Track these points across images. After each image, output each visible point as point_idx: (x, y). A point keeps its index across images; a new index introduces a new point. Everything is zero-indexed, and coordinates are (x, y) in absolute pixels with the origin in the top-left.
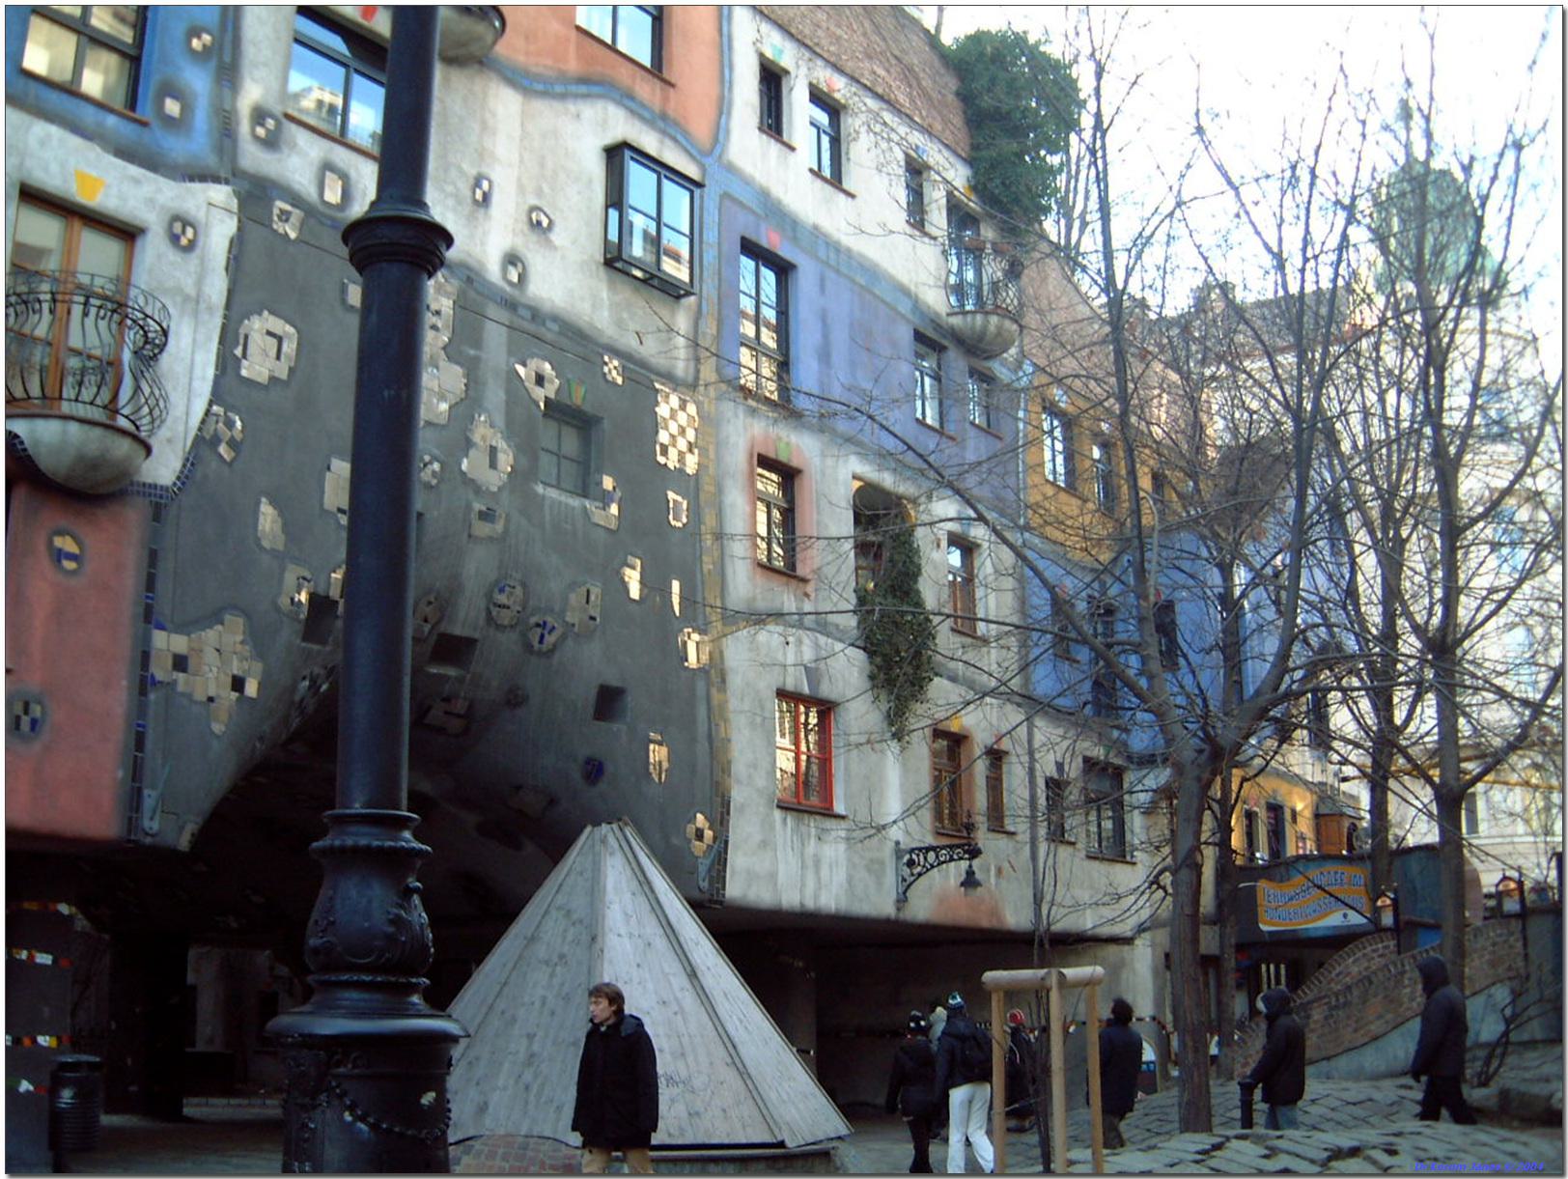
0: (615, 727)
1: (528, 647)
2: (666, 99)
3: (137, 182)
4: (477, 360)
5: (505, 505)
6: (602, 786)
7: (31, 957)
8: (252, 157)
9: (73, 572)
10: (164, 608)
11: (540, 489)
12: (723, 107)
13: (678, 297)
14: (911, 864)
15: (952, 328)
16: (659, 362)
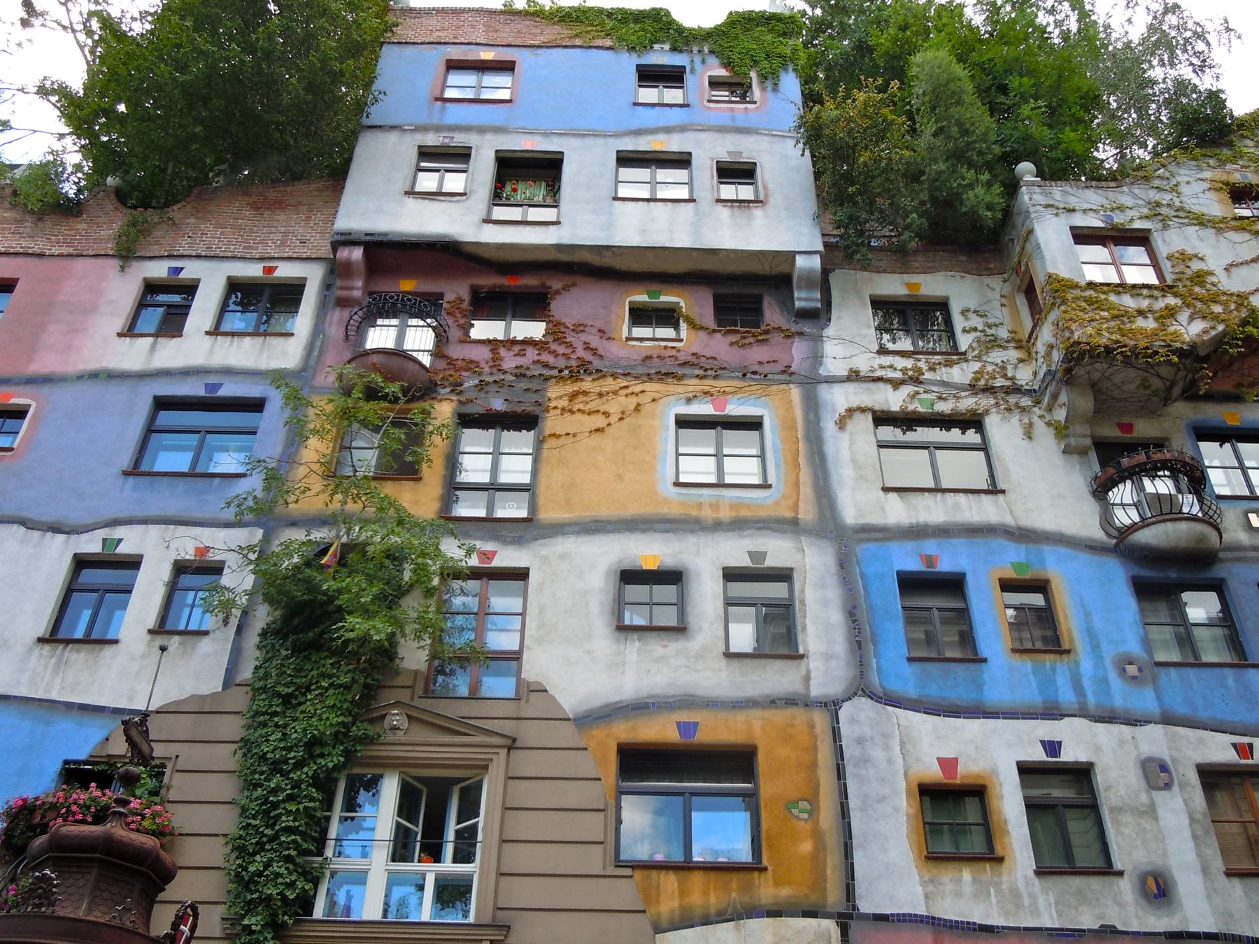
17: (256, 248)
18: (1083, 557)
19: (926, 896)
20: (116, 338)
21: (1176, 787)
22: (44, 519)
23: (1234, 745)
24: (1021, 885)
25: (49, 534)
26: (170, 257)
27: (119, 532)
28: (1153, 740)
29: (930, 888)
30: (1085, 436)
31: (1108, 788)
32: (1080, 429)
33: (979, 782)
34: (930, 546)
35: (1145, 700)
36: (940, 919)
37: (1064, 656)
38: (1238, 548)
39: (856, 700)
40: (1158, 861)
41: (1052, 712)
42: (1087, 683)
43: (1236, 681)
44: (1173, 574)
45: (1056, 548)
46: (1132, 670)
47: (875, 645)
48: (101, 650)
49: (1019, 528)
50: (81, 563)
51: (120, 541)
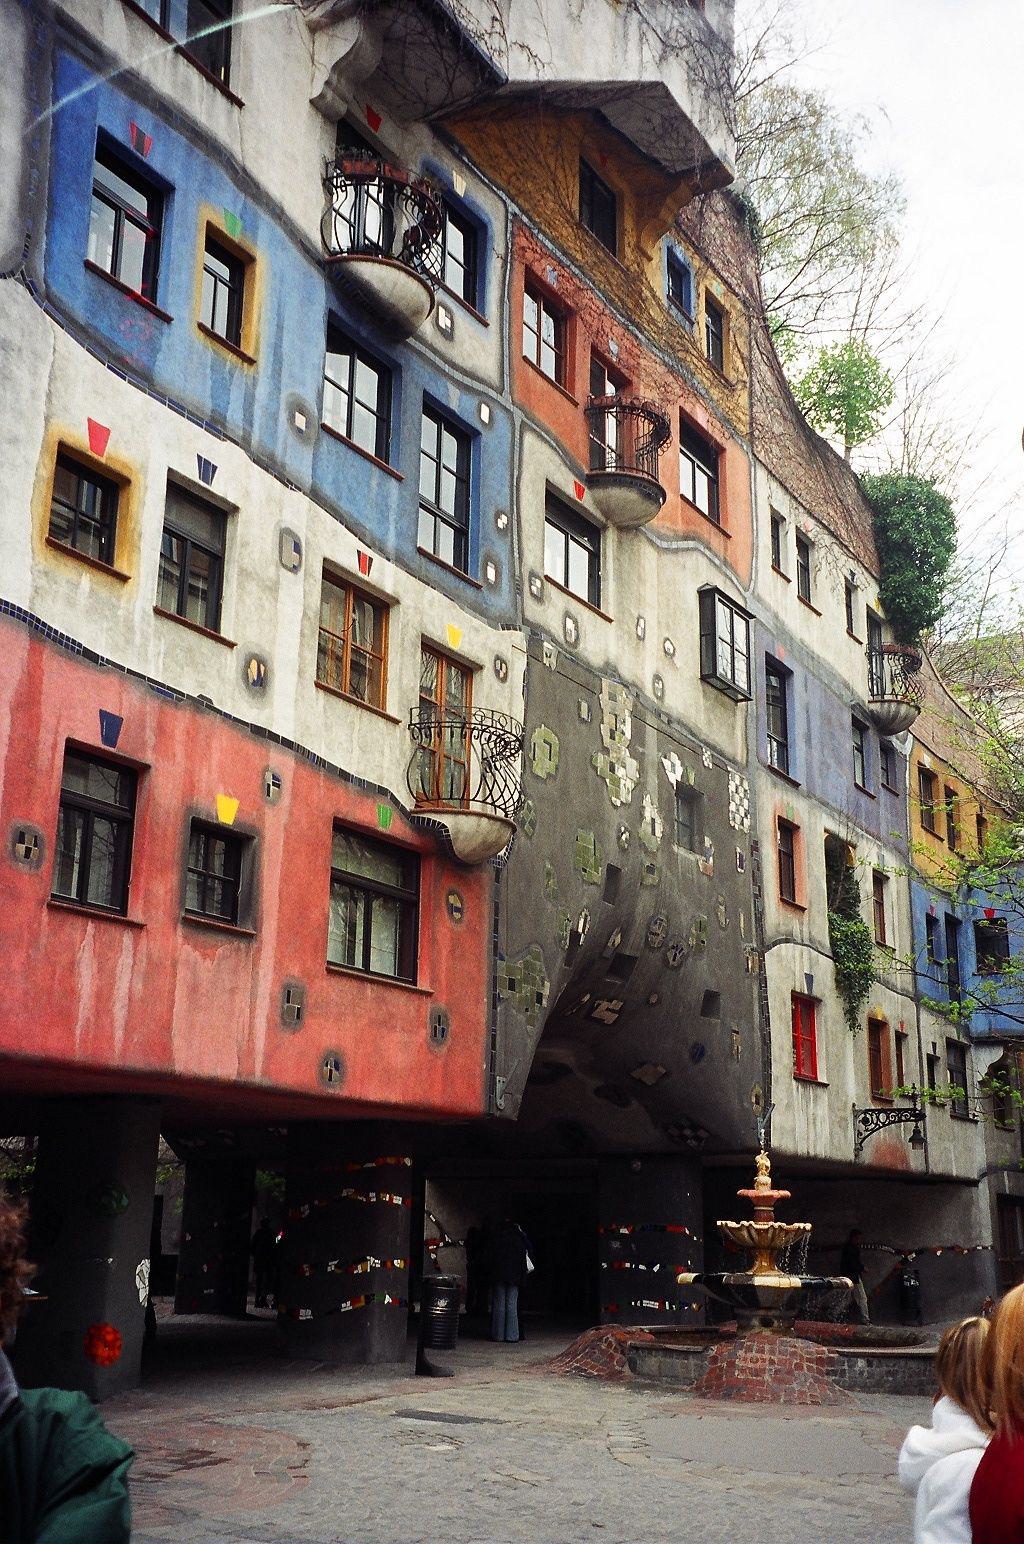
0: (714, 1021)
1: (665, 961)
2: (726, 549)
3: (477, 631)
4: (643, 754)
5: (660, 860)
6: (703, 1064)
7: (391, 1199)
8: (532, 610)
9: (459, 921)
10: (502, 946)
11: (675, 848)
12: (754, 549)
13: (737, 701)
14: (865, 1121)
15: (872, 711)
16: (728, 749)
18: (294, 253)
19: (36, 590)
21: (301, 573)
23: (359, 552)
24: (137, 618)
28: (298, 510)
29: (42, 582)
30: (344, 99)
31: (245, 545)
32: (344, 86)
33: (125, 473)
34: (146, 120)
35: (299, 461)
36: (44, 624)
37: (246, 364)
38: (421, 340)
39: (11, 281)
40: (264, 648)
41: (215, 426)
42: (258, 411)
43: (379, 485)
44: (364, 334)
45: (272, 222)
46: (300, 421)
47: (52, 215)
49: (244, 170)
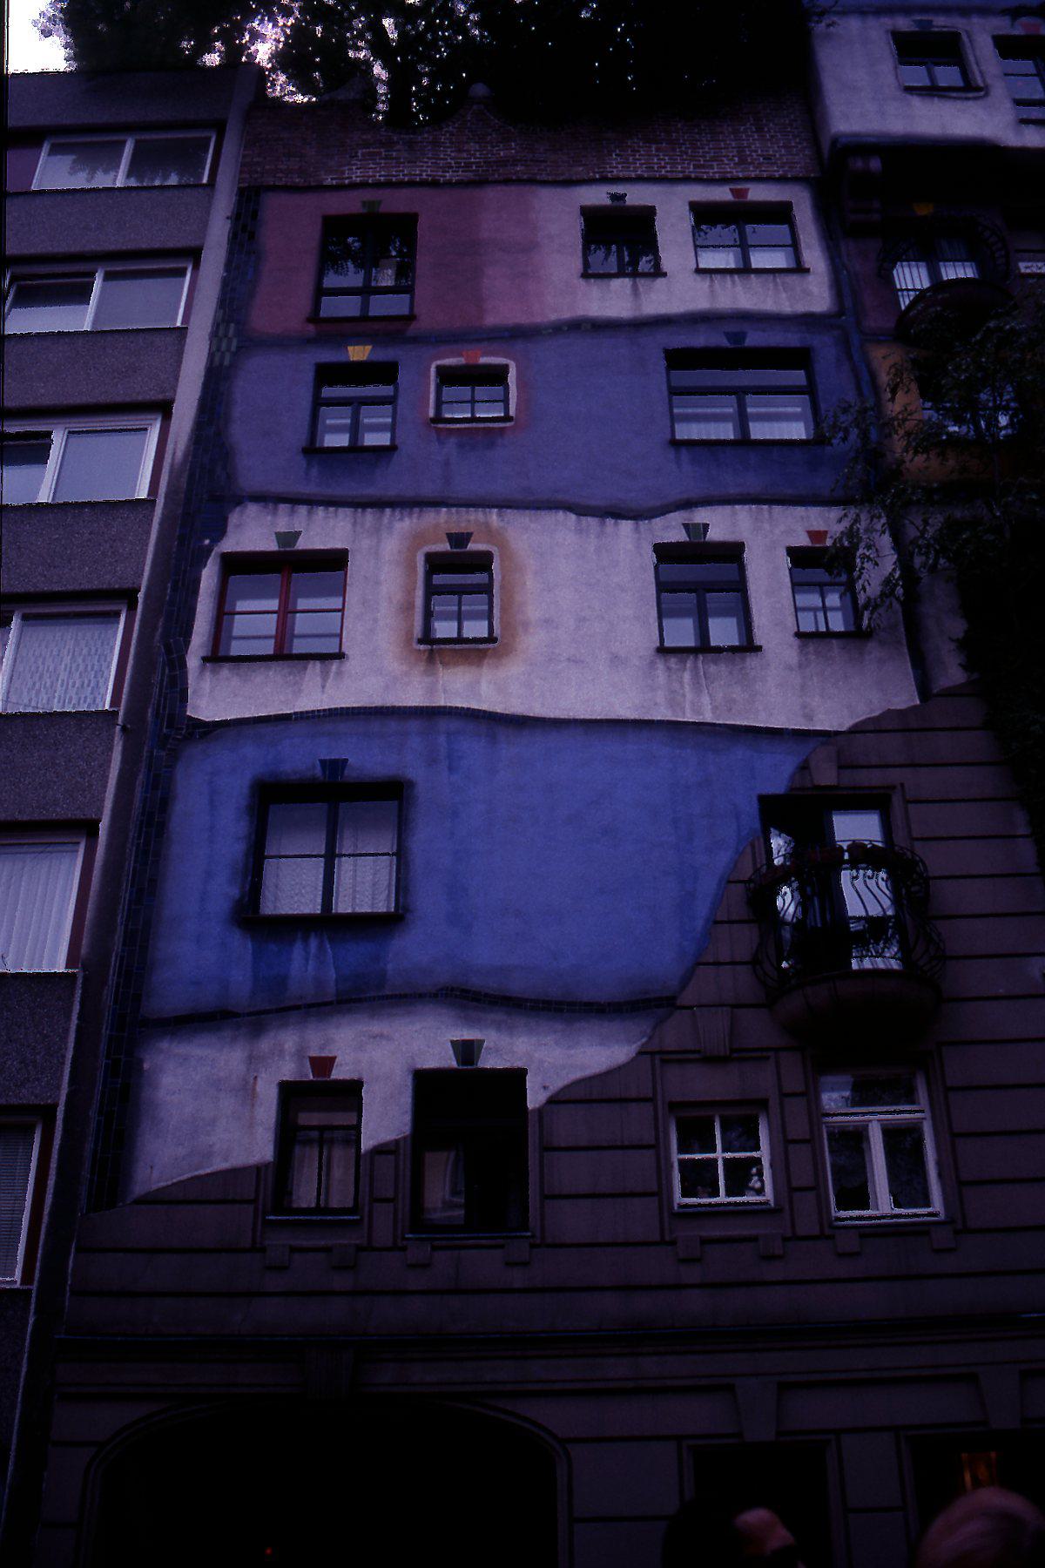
17: (711, 167)
20: (582, 282)
22: (593, 503)
25: (610, 522)
26: (604, 180)
27: (701, 516)
48: (743, 660)
50: (664, 553)
51: (706, 526)
